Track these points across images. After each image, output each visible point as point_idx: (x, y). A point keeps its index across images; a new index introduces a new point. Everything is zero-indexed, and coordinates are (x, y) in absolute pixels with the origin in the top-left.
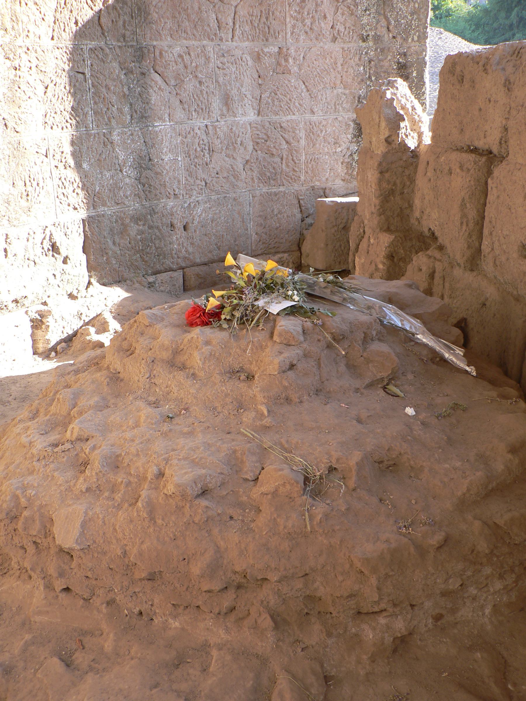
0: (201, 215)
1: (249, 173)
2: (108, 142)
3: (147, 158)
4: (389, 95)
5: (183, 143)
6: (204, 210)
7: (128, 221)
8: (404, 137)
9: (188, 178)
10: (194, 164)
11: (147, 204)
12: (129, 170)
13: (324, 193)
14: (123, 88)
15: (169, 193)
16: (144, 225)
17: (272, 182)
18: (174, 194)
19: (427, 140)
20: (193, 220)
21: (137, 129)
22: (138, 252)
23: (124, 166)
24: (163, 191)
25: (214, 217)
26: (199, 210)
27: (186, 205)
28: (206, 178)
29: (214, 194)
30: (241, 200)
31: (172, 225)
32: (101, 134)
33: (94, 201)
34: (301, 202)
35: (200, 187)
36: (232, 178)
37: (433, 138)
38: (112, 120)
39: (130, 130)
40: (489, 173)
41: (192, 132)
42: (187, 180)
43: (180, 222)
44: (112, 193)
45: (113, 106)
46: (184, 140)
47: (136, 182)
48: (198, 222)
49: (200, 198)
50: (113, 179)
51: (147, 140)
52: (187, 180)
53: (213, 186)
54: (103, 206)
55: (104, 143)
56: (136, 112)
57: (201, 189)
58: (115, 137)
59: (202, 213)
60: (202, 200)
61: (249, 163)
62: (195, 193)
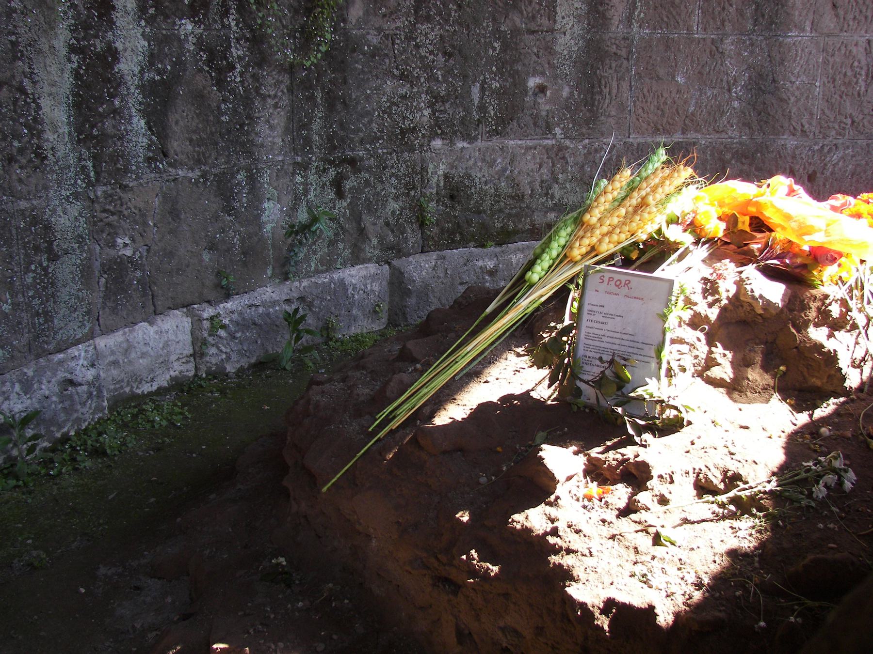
0: (837, 163)
2: (716, 52)
3: (771, 77)
5: (826, 62)
6: (842, 158)
7: (728, 156)
9: (826, 111)
10: (839, 93)
11: (759, 138)
12: (740, 91)
15: (794, 128)
18: (802, 131)
20: (824, 169)
21: (760, 38)
23: (734, 84)
24: (786, 125)
25: (855, 169)
26: (835, 157)
27: (816, 148)
28: (854, 114)
29: (862, 137)
32: (709, 42)
33: (685, 124)
35: (842, 125)
39: (750, 39)
41: (843, 48)
42: (823, 113)
43: (804, 169)
44: (712, 118)
45: (731, 5)
46: (829, 58)
47: (749, 107)
48: (832, 173)
49: (841, 141)
50: (716, 100)
51: (773, 54)
52: (823, 113)
53: (863, 126)
54: (696, 131)
55: (711, 52)
56: (763, 16)
57: (844, 129)
58: (728, 46)
59: (839, 161)
60: (843, 144)
62: (833, 133)
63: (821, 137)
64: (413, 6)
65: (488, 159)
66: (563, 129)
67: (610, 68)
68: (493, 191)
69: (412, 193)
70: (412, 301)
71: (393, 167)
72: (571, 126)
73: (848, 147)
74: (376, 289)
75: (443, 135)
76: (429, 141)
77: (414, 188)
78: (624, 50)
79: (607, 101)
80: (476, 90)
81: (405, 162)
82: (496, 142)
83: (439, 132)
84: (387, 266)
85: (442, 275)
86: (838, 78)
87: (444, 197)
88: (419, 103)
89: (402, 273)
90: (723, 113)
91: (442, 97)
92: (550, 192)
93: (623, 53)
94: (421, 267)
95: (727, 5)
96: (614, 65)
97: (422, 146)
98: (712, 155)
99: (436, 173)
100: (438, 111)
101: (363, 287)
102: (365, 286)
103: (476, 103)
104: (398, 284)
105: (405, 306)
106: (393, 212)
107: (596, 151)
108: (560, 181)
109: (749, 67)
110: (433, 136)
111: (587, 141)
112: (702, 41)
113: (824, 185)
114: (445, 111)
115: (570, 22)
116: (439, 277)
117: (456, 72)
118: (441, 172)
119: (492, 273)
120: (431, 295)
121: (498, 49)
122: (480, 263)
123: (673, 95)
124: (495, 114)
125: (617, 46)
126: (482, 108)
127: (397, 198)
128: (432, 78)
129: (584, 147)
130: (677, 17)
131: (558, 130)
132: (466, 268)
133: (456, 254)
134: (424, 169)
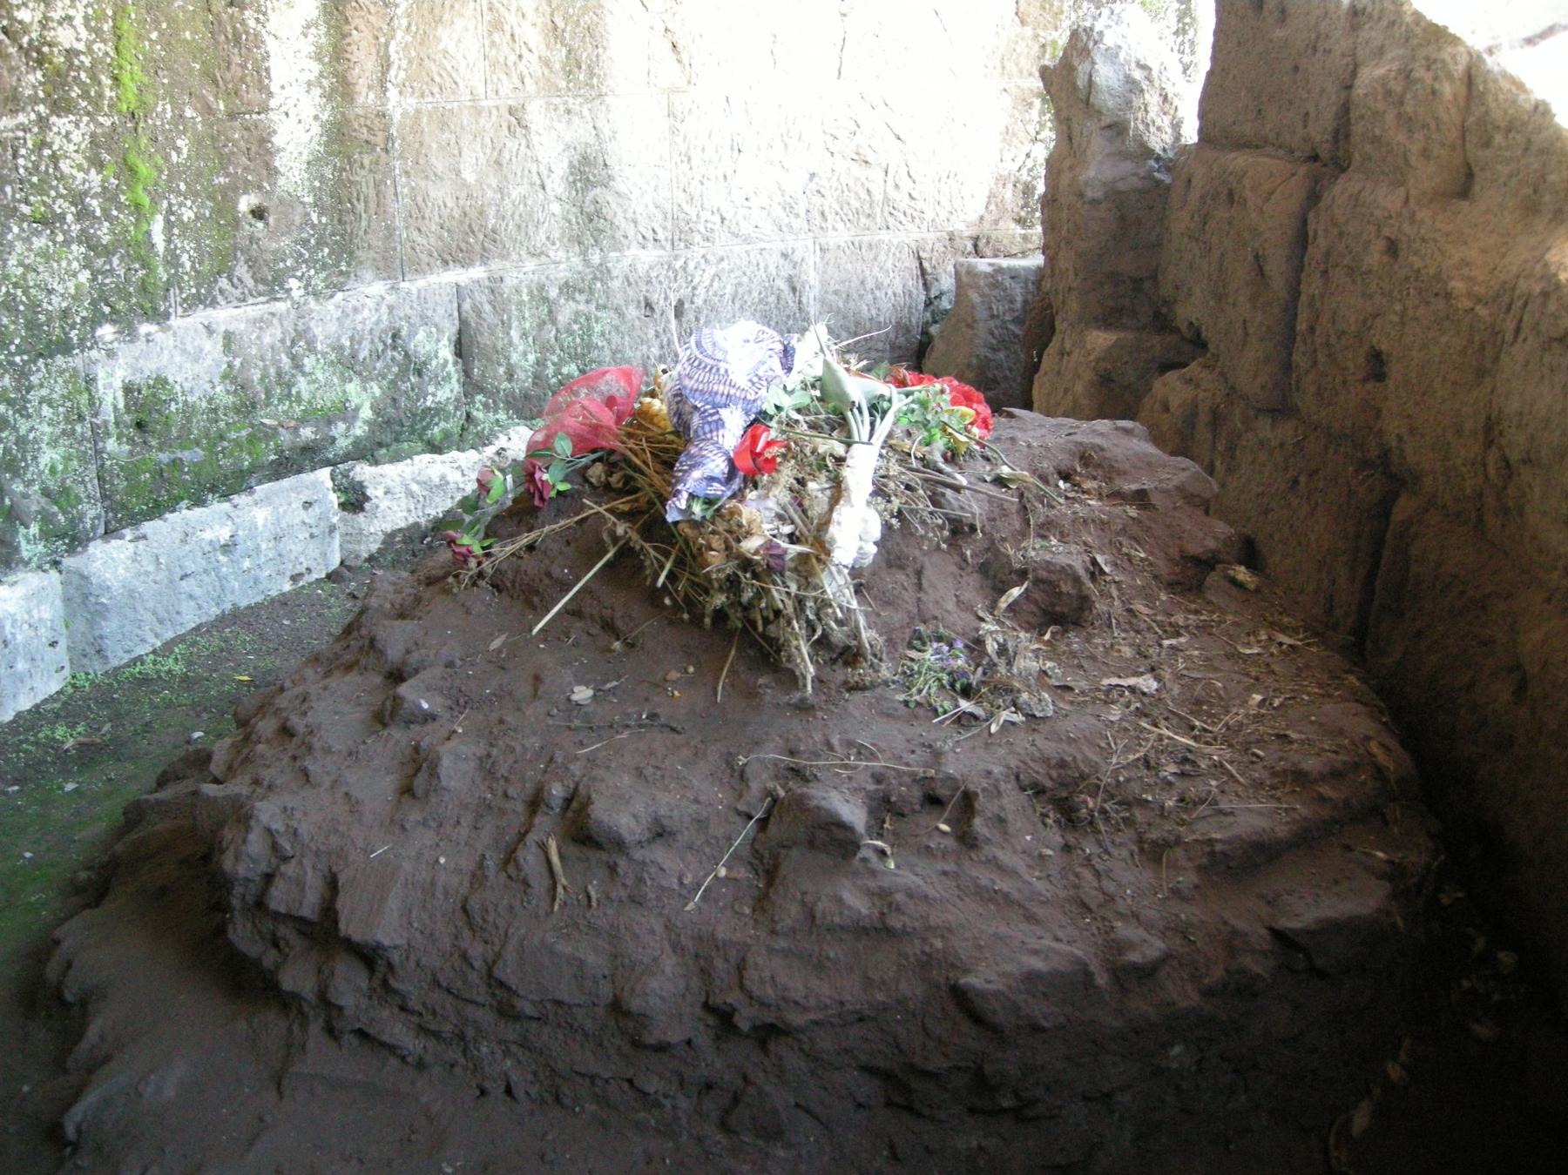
1: (817, 200)
4: (1109, 40)
6: (717, 276)
8: (1141, 127)
9: (684, 206)
13: (975, 246)
14: (552, 14)
16: (587, 302)
17: (863, 220)
19: (1190, 135)
21: (580, 100)
22: (574, 357)
24: (631, 232)
29: (739, 241)
30: (797, 257)
31: (648, 305)
34: (926, 265)
35: (710, 225)
36: (778, 212)
37: (1201, 131)
38: (527, 80)
40: (1313, 198)
46: (678, 125)
61: (816, 179)
63: (682, 245)
64: (41, 83)
65: (189, 348)
66: (300, 279)
67: (362, 166)
68: (204, 405)
69: (78, 428)
70: (109, 627)
71: (41, 386)
72: (312, 272)
73: (722, 259)
74: (47, 616)
75: (115, 317)
76: (93, 330)
77: (81, 418)
78: (380, 134)
79: (364, 223)
80: (157, 227)
81: (62, 372)
82: (202, 315)
83: (107, 310)
84: (54, 574)
85: (151, 568)
86: (693, 156)
87: (127, 427)
88: (69, 264)
89: (84, 577)
90: (538, 224)
91: (105, 247)
92: (294, 391)
93: (379, 139)
94: (111, 560)
95: (525, 52)
96: (366, 162)
97: (82, 340)
98: (530, 293)
99: (110, 385)
100: (103, 273)
101: (26, 617)
102: (29, 612)
103: (160, 246)
104: (83, 600)
105: (101, 637)
106: (53, 470)
107: (356, 310)
108: (307, 369)
109: (568, 147)
110: (96, 320)
111: (340, 296)
112: (494, 112)
113: (697, 319)
114: (112, 271)
115: (298, 91)
116: (147, 573)
117: (123, 198)
118: (118, 384)
119: (227, 548)
120: (140, 608)
121: (185, 150)
122: (208, 535)
123: (461, 202)
124: (193, 267)
125: (370, 129)
126: (172, 260)
127: (56, 441)
128: (83, 214)
129: (338, 307)
130: (454, 74)
131: (293, 283)
132: (187, 548)
133: (159, 530)
134: (90, 381)
